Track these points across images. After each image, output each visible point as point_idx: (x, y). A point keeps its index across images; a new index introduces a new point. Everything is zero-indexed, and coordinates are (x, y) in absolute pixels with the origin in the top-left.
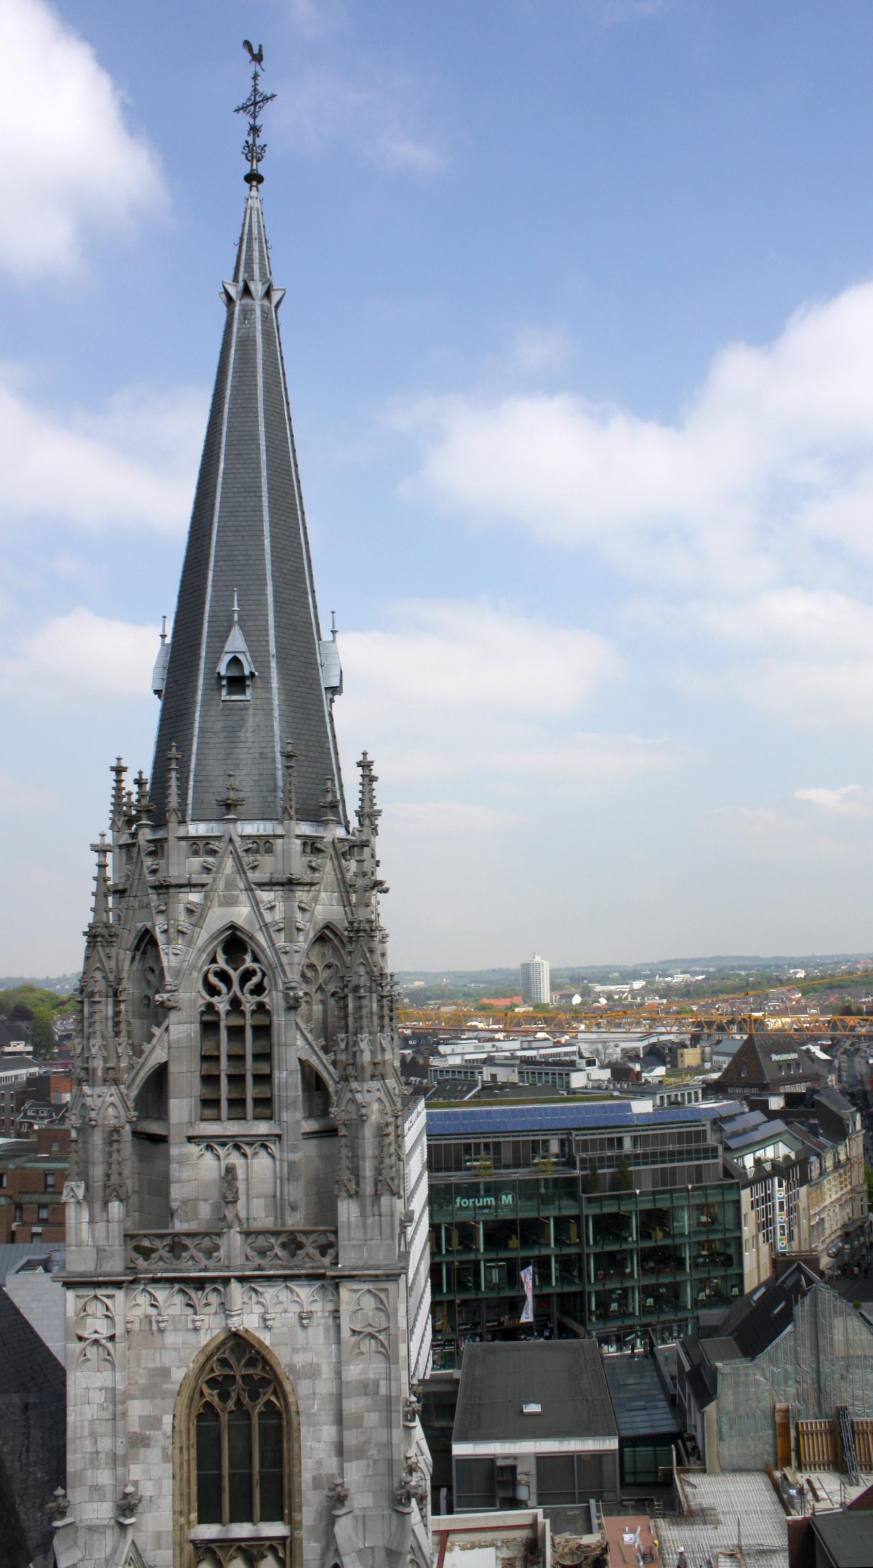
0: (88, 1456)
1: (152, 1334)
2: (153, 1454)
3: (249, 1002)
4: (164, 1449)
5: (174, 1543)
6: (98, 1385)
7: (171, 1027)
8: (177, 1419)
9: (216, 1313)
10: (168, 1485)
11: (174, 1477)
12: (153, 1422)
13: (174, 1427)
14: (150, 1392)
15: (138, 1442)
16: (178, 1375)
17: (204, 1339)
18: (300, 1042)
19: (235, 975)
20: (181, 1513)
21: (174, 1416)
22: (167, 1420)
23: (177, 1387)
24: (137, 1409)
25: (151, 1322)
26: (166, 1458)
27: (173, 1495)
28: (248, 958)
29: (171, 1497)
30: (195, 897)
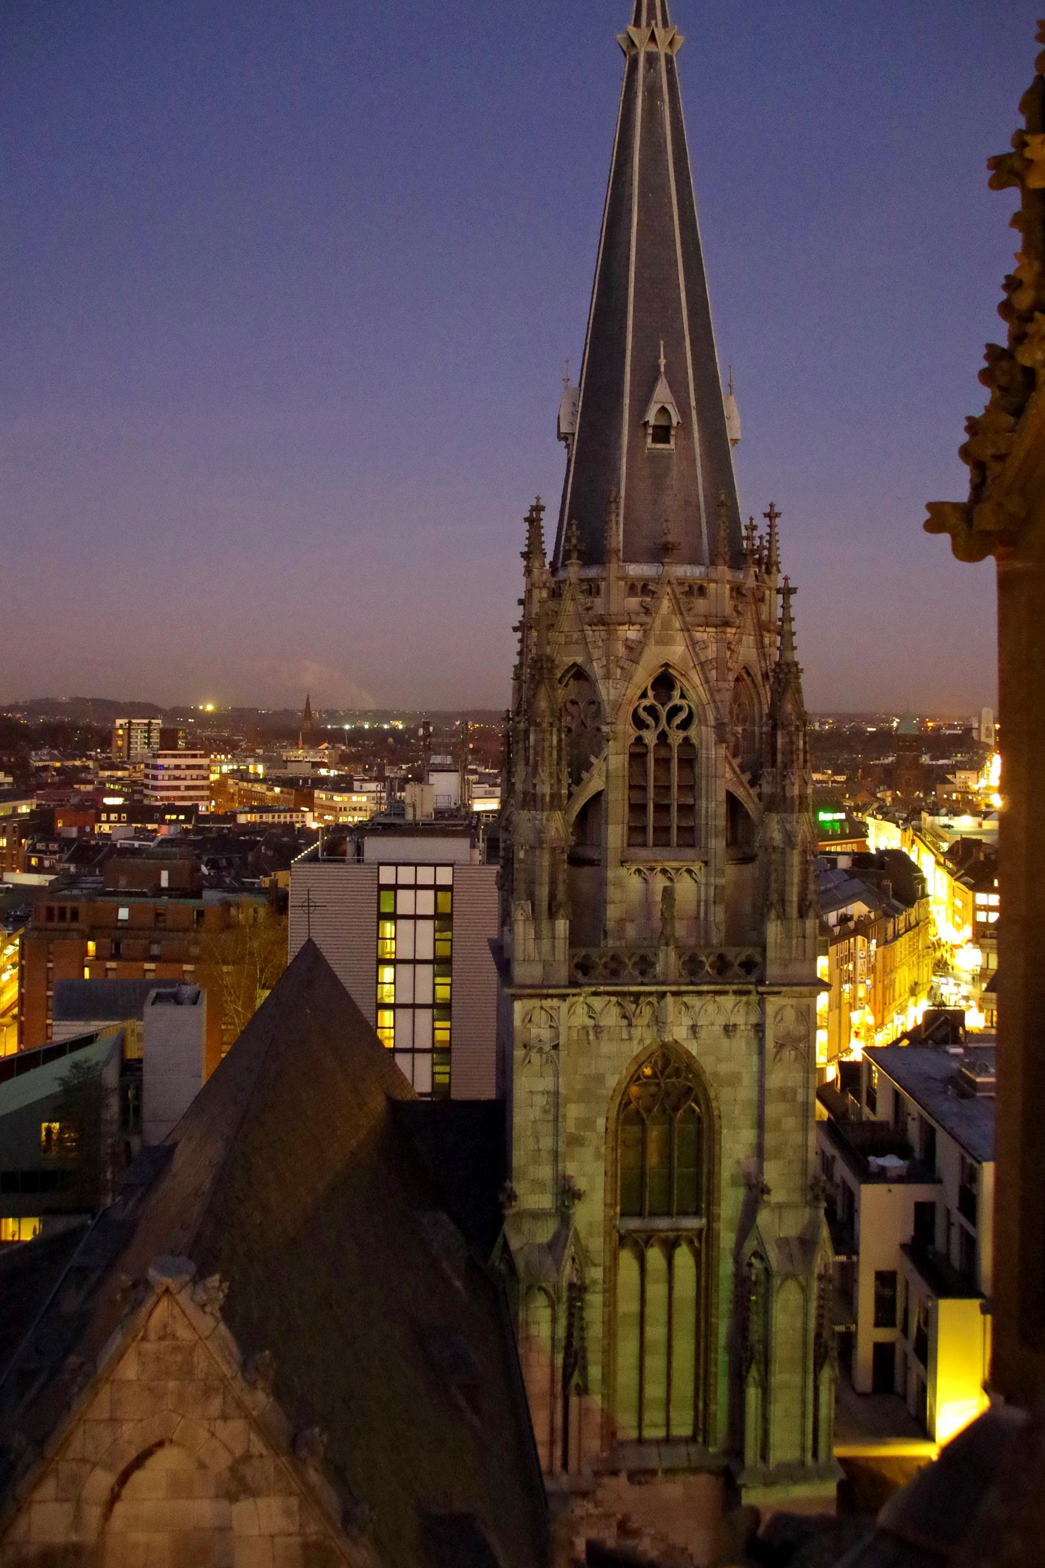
0: (530, 1153)
1: (589, 1043)
2: (587, 1153)
3: (676, 737)
4: (597, 1148)
5: (605, 1232)
6: (541, 1089)
7: (610, 757)
8: (609, 1121)
9: (648, 1026)
10: (600, 1181)
11: (606, 1174)
12: (586, 1123)
13: (607, 1129)
14: (585, 1096)
15: (576, 1141)
16: (612, 1082)
17: (636, 1048)
18: (729, 775)
19: (663, 712)
20: (611, 1205)
21: (607, 1119)
22: (601, 1122)
23: (611, 1093)
24: (573, 1111)
25: (588, 1033)
26: (598, 1156)
27: (605, 1190)
28: (676, 693)
29: (602, 1191)
30: (632, 633)
